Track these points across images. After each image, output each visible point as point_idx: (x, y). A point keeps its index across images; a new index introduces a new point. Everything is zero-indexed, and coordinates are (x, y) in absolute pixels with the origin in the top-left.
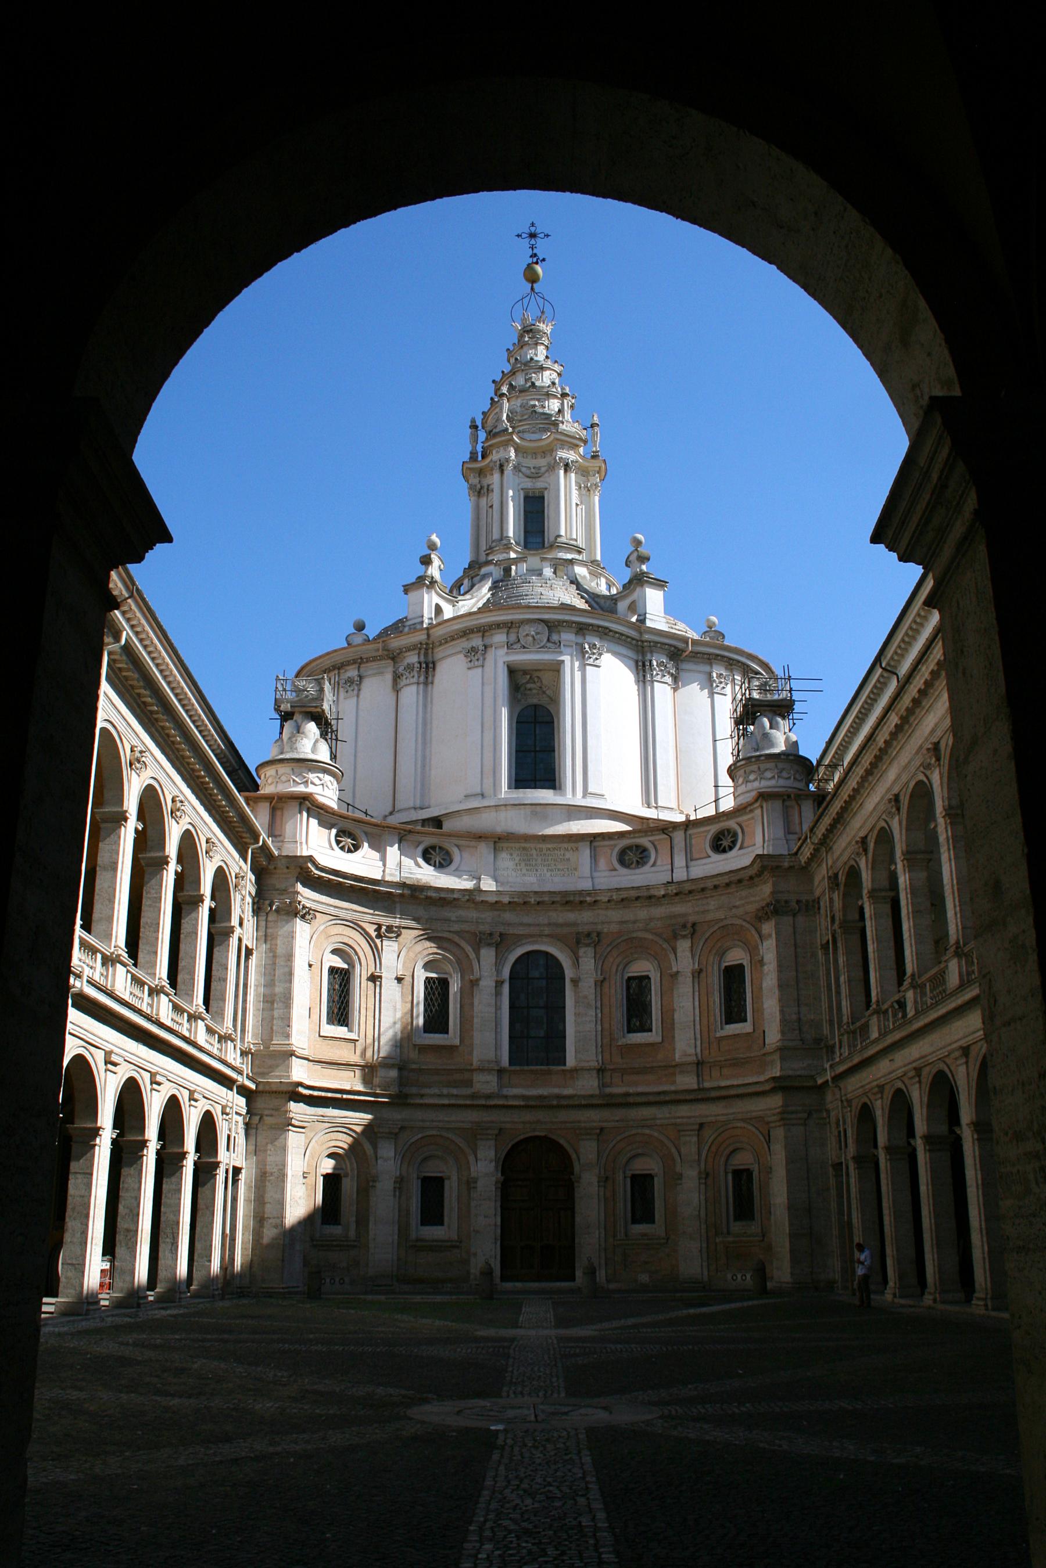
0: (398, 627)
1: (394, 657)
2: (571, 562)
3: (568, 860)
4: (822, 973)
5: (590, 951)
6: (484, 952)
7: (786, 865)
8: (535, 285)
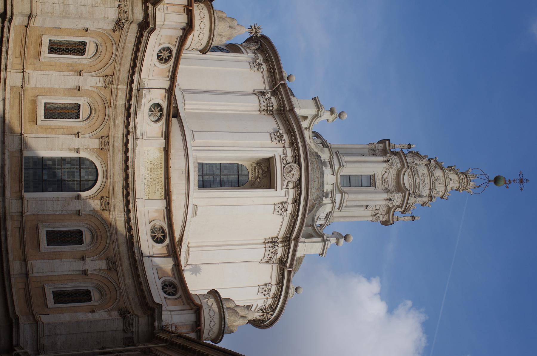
2: (333, 202)
3: (155, 194)
7: (156, 324)
8: (493, 183)
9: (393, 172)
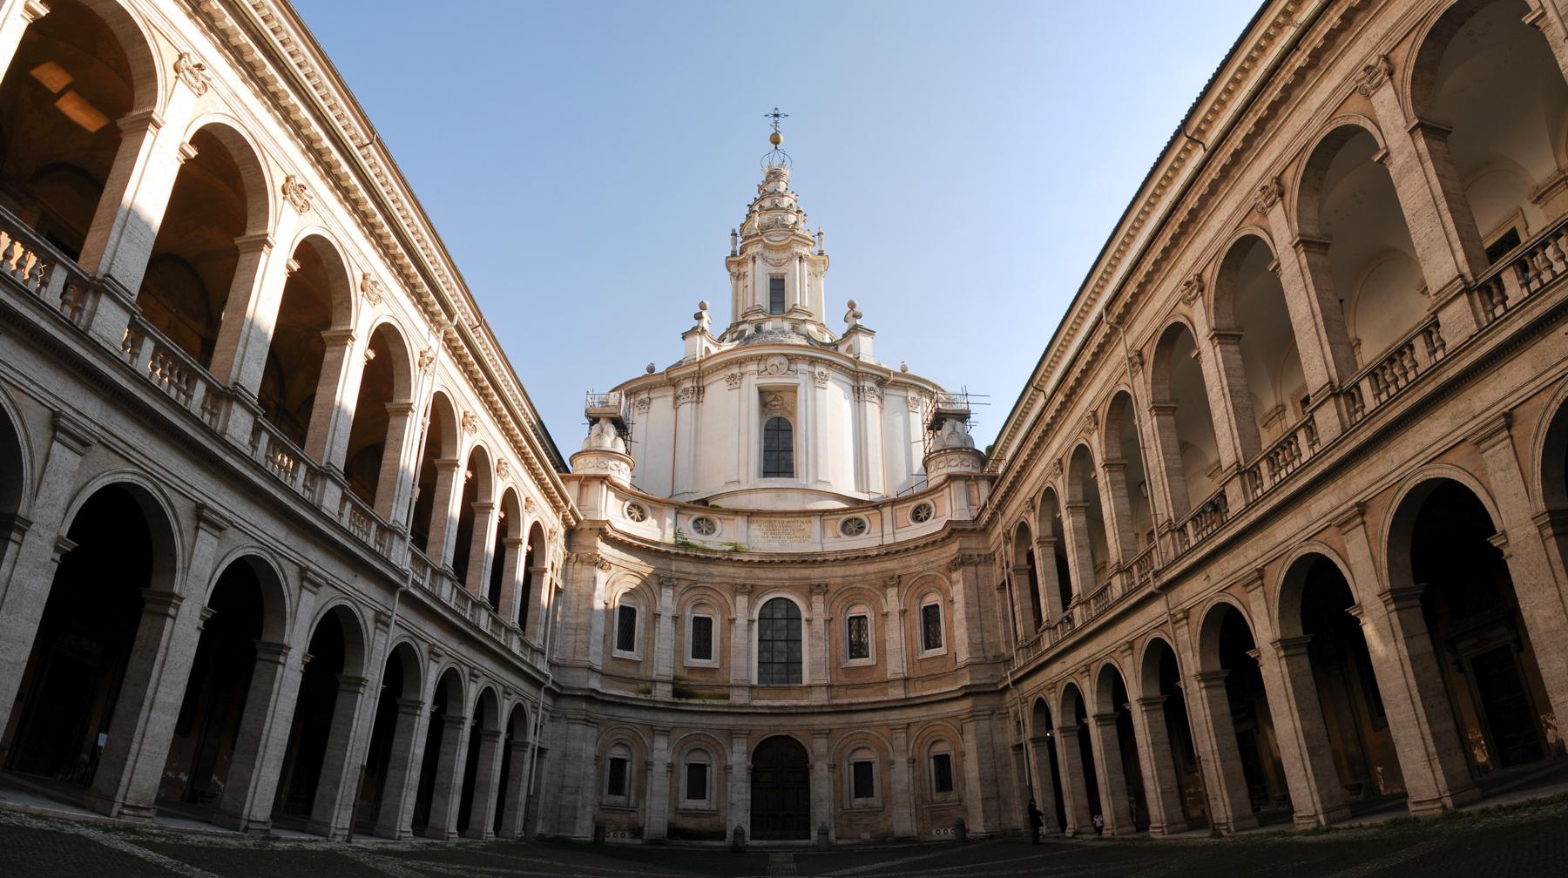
0: (679, 365)
1: (674, 383)
4: (998, 607)
5: (821, 598)
6: (739, 598)
7: (970, 527)
9: (767, 253)
